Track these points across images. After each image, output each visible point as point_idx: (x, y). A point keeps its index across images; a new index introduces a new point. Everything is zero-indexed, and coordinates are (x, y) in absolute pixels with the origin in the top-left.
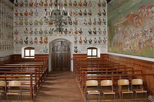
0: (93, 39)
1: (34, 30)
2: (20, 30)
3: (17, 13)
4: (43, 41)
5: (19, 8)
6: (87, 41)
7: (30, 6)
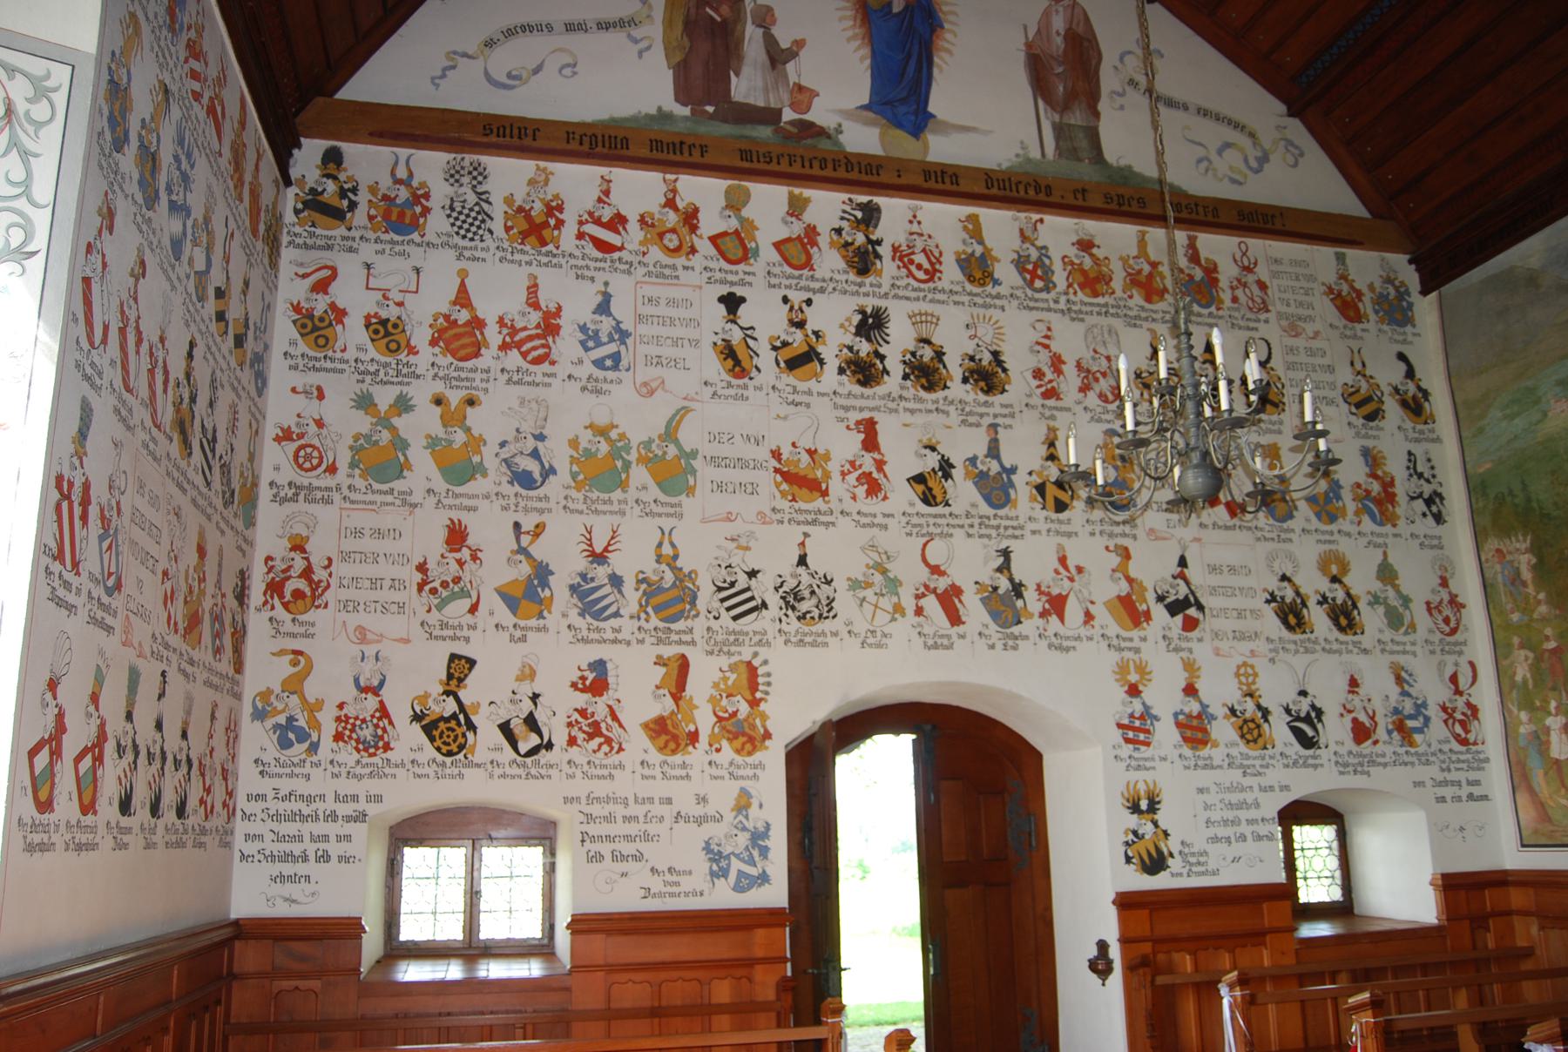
0: (1330, 696)
1: (567, 563)
2: (349, 544)
3: (320, 304)
4: (704, 721)
5: (367, 251)
6: (1266, 713)
7: (525, 235)
